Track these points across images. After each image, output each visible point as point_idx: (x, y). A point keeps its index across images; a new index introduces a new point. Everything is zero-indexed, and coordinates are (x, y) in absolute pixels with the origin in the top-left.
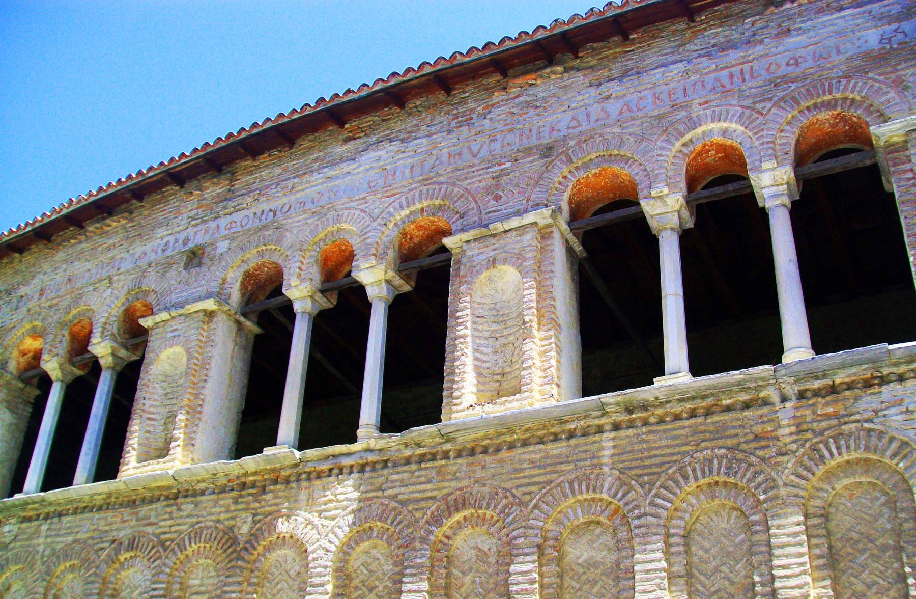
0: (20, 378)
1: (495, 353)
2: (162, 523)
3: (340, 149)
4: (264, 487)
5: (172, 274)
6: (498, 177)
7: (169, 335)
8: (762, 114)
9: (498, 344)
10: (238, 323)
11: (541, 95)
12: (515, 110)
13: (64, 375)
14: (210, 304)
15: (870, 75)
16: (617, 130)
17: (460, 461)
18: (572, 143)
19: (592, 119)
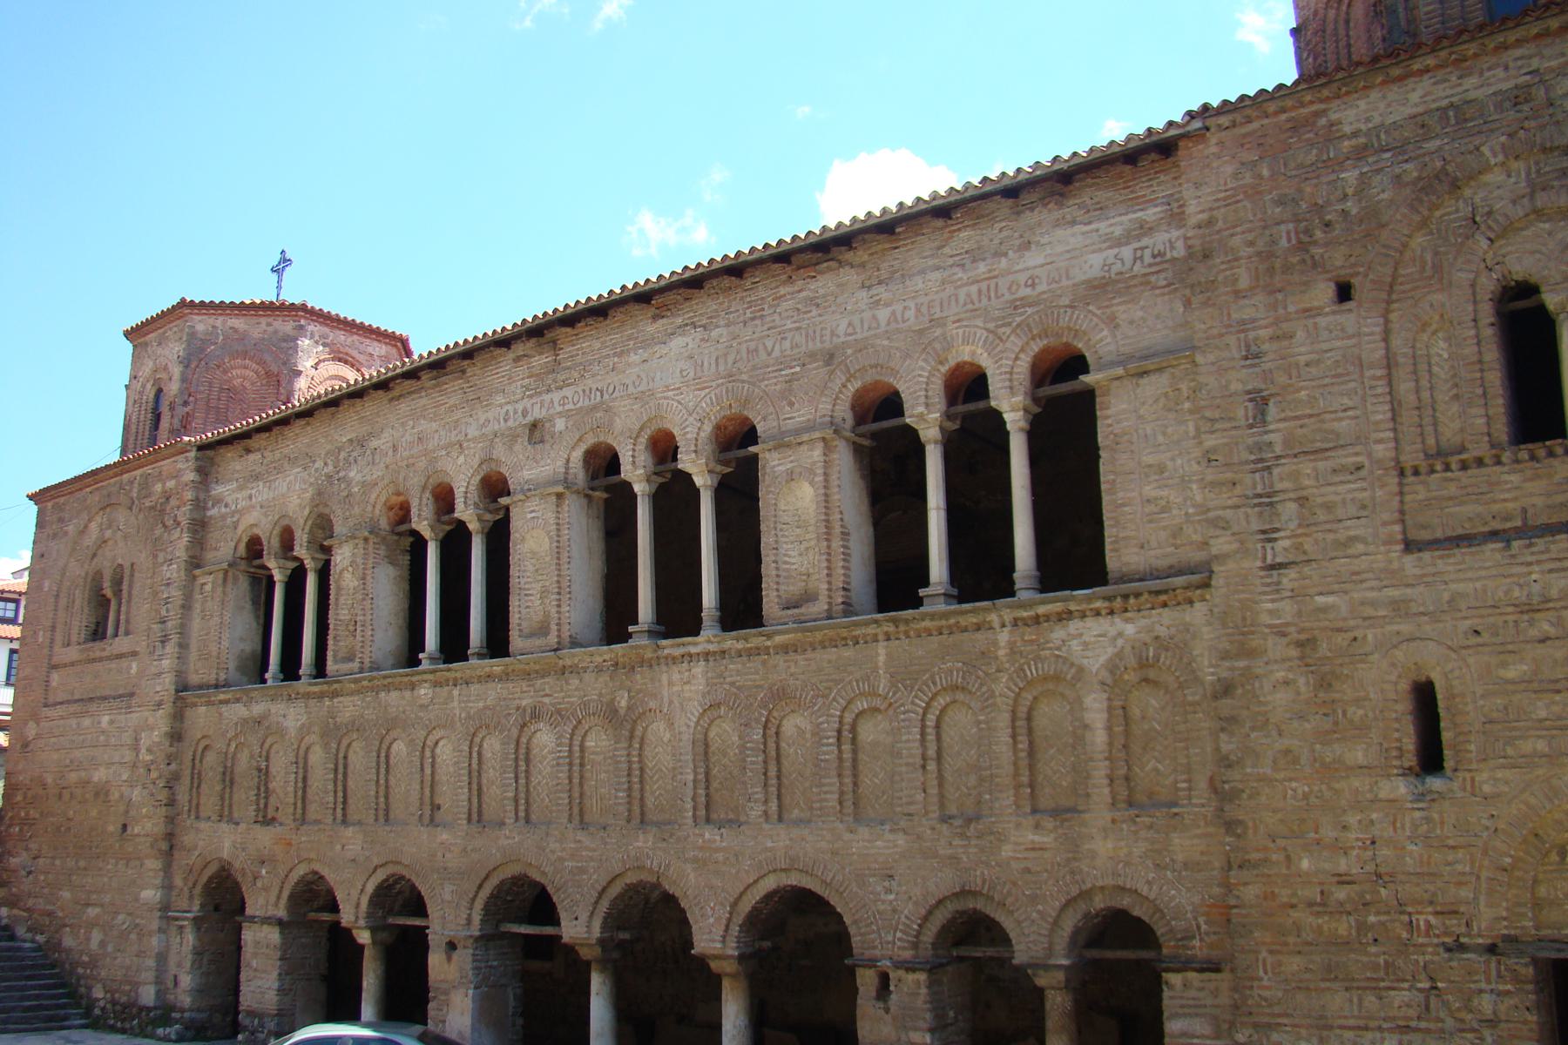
0: (393, 532)
1: (800, 555)
3: (651, 328)
4: (633, 668)
5: (517, 447)
6: (790, 381)
7: (529, 516)
8: (1001, 340)
9: (803, 547)
10: (587, 496)
11: (821, 291)
12: (799, 306)
13: (436, 535)
14: (560, 489)
15: (1091, 308)
16: (886, 342)
17: (778, 657)
18: (849, 351)
19: (866, 326)
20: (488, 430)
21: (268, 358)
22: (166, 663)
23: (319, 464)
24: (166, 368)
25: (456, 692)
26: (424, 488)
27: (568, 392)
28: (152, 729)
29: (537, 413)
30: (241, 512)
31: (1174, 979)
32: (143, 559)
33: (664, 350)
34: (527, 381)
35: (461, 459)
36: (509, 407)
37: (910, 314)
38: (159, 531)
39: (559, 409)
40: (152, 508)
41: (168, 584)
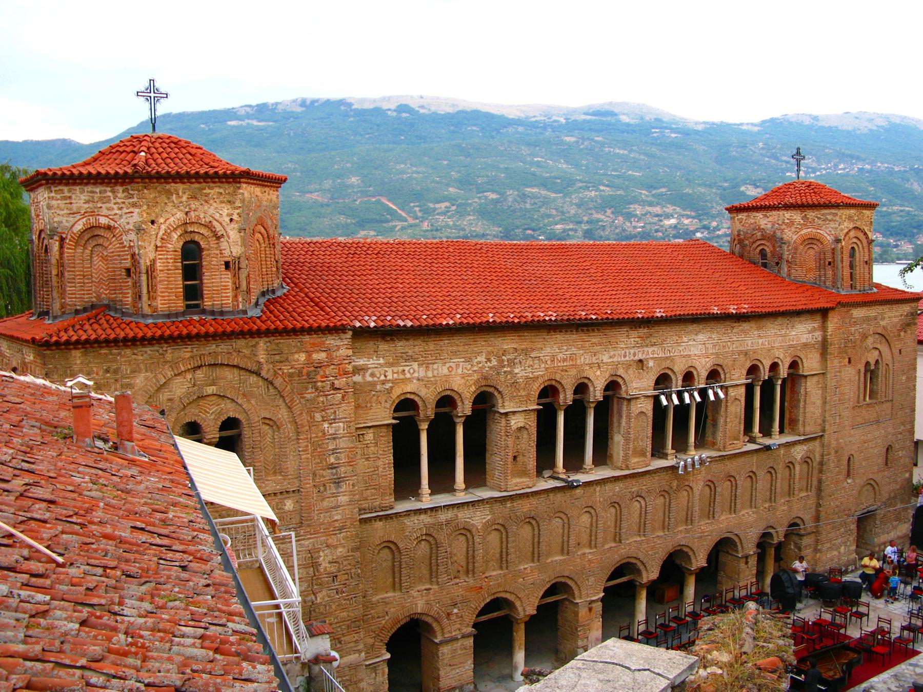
5: (630, 371)
20: (615, 359)
21: (269, 223)
22: (343, 499)
23: (482, 358)
24: (209, 226)
25: (598, 489)
26: (573, 385)
27: (655, 348)
28: (336, 547)
29: (640, 356)
30: (394, 382)
31: (805, 537)
32: (283, 414)
33: (695, 338)
34: (637, 339)
35: (598, 373)
36: (627, 351)
37: (766, 343)
38: (310, 394)
39: (651, 356)
40: (291, 375)
41: (334, 439)
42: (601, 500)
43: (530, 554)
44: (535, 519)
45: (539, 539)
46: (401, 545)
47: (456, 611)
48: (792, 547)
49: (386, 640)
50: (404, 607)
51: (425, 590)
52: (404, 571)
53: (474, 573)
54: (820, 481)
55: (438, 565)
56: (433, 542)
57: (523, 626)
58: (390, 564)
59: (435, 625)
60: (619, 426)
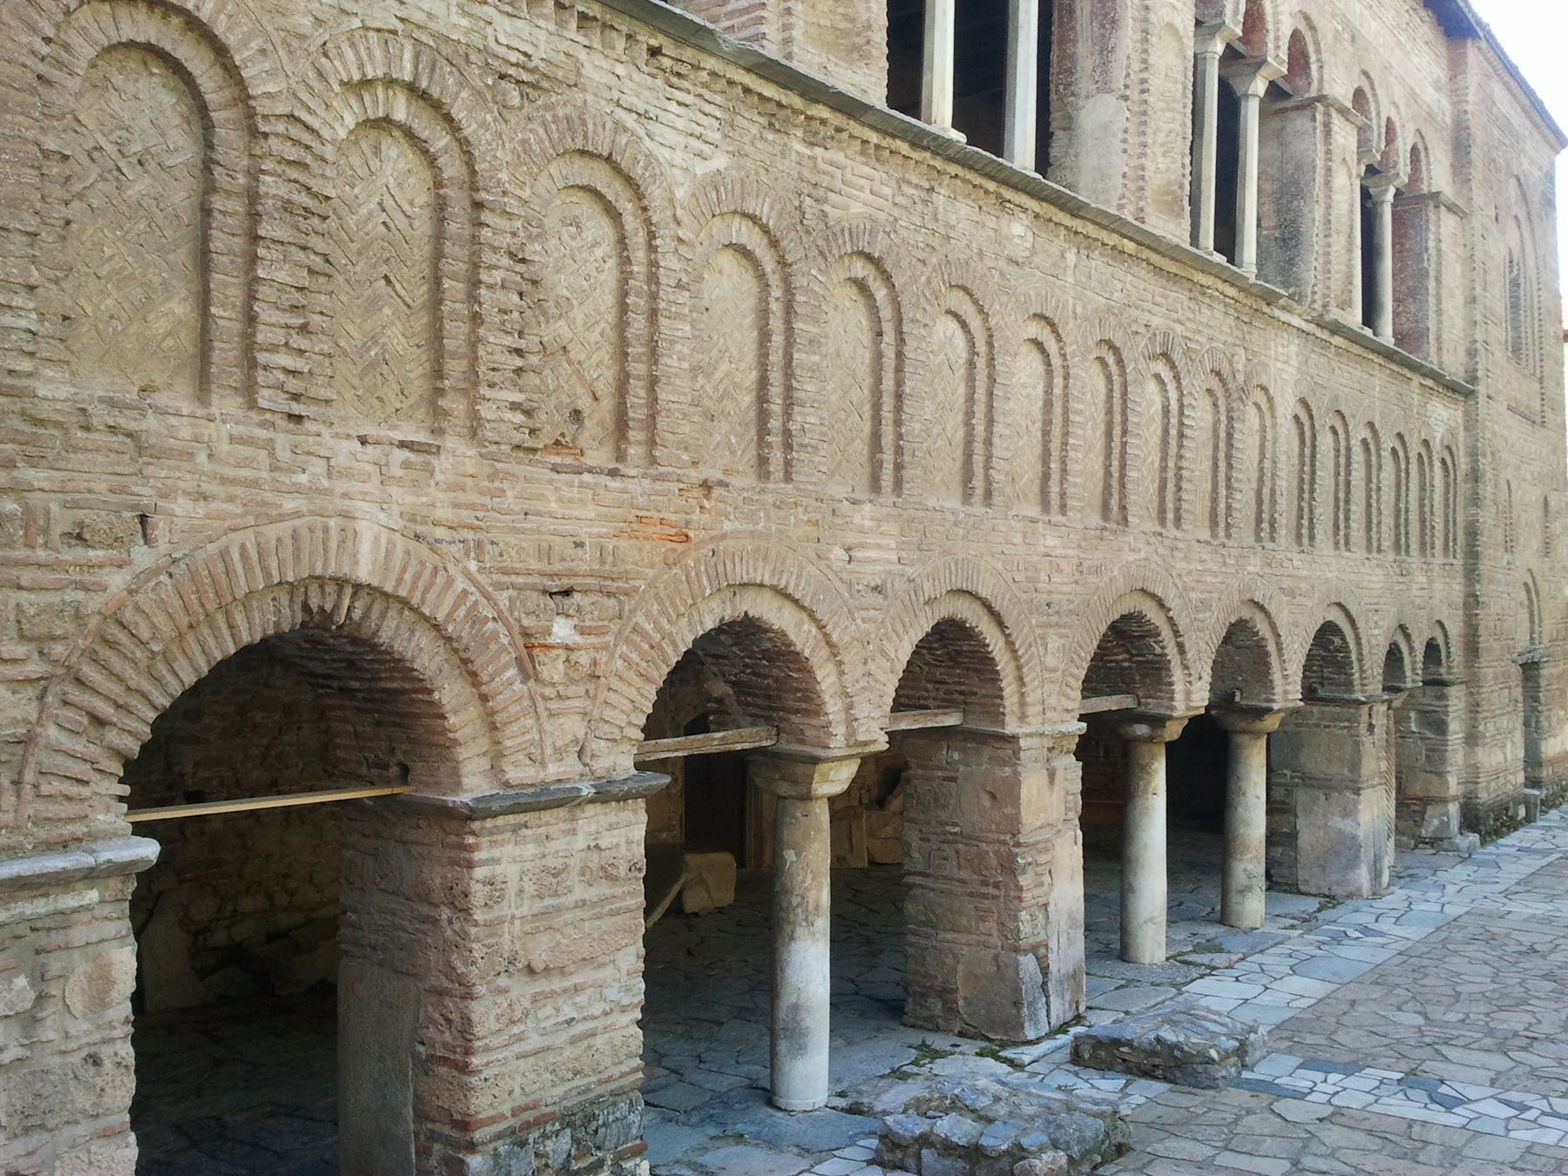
2: (1189, 325)
42: (1079, 310)
43: (860, 447)
44: (887, 278)
45: (899, 383)
46: (263, 82)
47: (562, 630)
48: (1414, 728)
49: (132, 734)
50: (266, 514)
51: (403, 445)
52: (276, 271)
53: (652, 443)
54: (1472, 532)
55: (476, 319)
56: (452, 168)
57: (822, 813)
58: (181, 197)
59: (451, 693)
60: (1105, 51)
